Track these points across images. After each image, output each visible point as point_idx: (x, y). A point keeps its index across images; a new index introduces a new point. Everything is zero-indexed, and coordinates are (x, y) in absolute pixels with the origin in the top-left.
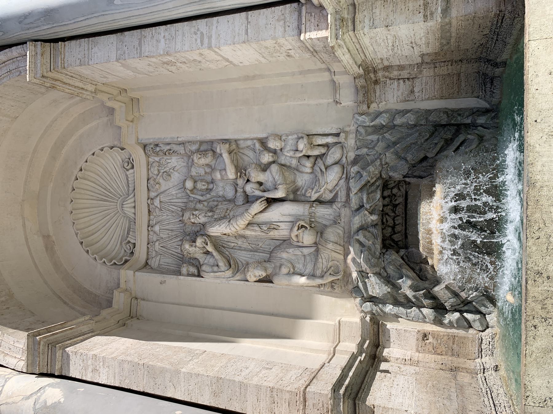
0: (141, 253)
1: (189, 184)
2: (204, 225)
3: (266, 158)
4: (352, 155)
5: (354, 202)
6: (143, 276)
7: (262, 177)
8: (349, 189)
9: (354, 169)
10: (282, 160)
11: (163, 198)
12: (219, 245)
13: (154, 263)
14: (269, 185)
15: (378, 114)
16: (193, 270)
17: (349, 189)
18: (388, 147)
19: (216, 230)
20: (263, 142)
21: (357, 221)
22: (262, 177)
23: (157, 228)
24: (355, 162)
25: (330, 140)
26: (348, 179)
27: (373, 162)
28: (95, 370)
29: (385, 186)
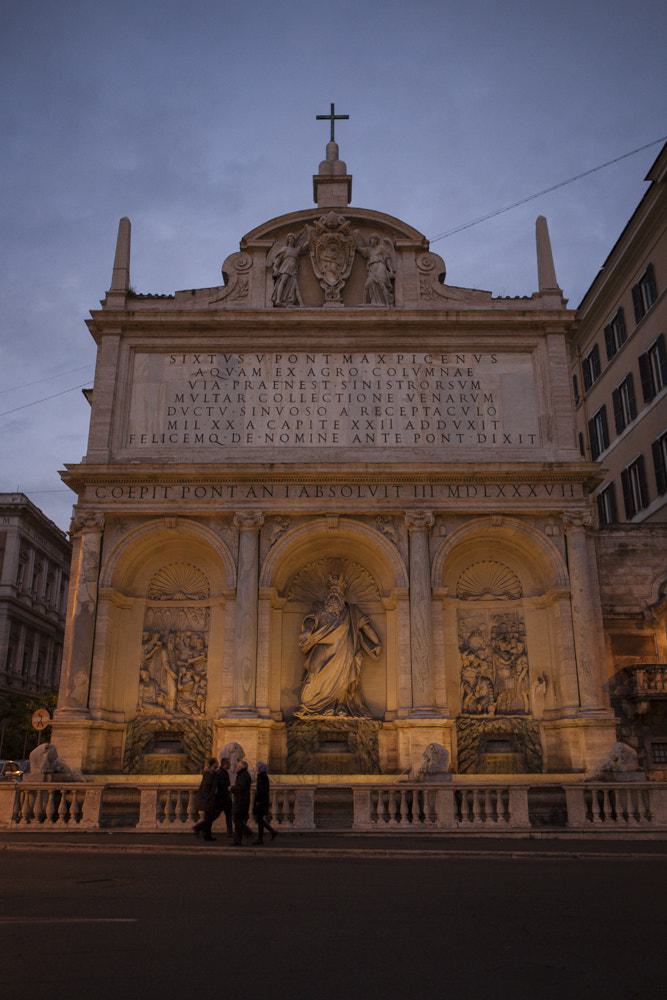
0: (154, 604)
1: (189, 633)
2: (166, 647)
3: (197, 678)
4: (195, 718)
5: (172, 721)
6: (143, 610)
7: (188, 676)
8: (179, 718)
9: (187, 720)
10: (196, 686)
11: (184, 616)
12: (158, 653)
13: (150, 613)
14: (184, 680)
15: (211, 730)
16: (146, 638)
17: (179, 718)
18: (196, 734)
19: (164, 653)
20: (204, 677)
21: (165, 722)
22: (188, 676)
23: (168, 613)
24: (192, 721)
25: (202, 709)
26: (183, 718)
27: (190, 727)
28: (101, 621)
29: (183, 733)
